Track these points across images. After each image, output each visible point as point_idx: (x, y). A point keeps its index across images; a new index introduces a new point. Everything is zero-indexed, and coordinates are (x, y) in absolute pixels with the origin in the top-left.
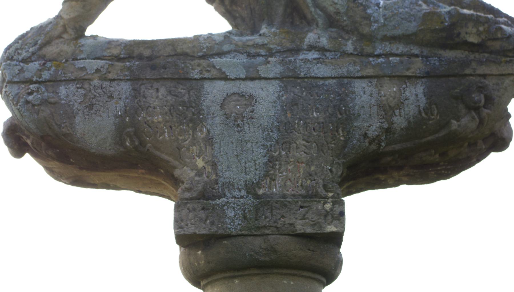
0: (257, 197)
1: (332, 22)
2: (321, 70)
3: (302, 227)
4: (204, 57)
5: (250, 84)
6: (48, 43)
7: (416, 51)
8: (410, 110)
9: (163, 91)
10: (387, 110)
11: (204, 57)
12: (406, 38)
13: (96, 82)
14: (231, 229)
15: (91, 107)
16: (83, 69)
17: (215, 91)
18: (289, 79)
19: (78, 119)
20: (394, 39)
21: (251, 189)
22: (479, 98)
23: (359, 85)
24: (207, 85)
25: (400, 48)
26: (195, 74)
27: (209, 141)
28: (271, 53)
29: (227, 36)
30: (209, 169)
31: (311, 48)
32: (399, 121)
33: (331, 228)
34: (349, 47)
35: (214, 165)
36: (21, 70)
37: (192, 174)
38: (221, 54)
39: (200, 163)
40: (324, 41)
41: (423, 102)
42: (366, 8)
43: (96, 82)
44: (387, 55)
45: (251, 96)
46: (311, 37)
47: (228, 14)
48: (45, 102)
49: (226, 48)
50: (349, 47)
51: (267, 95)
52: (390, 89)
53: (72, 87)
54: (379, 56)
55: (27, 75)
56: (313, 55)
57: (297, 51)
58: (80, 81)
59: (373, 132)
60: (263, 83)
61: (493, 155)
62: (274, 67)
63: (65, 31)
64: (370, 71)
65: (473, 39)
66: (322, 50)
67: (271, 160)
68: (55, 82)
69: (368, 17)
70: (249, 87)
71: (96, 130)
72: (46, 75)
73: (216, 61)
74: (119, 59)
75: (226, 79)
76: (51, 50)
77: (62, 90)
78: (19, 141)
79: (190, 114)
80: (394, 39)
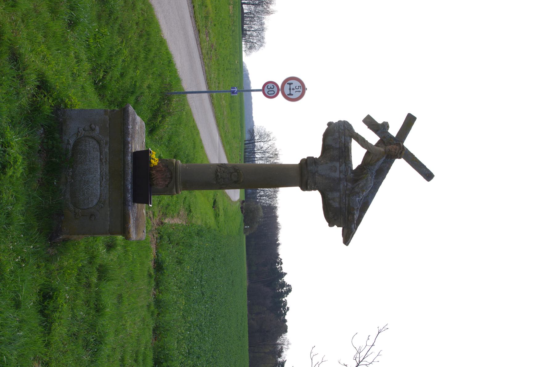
1: (353, 188)
2: (342, 186)
3: (309, 181)
12: (349, 204)
17: (337, 164)
18: (340, 179)
21: (317, 172)
23: (338, 194)
25: (347, 203)
27: (327, 163)
28: (345, 176)
29: (351, 167)
32: (331, 202)
33: (308, 187)
34: (347, 192)
38: (346, 166)
40: (349, 187)
46: (350, 184)
47: (359, 167)
50: (347, 192)
51: (337, 175)
57: (346, 181)
58: (339, 137)
70: (338, 172)
73: (344, 165)
74: (345, 144)
76: (347, 131)
78: (330, 124)
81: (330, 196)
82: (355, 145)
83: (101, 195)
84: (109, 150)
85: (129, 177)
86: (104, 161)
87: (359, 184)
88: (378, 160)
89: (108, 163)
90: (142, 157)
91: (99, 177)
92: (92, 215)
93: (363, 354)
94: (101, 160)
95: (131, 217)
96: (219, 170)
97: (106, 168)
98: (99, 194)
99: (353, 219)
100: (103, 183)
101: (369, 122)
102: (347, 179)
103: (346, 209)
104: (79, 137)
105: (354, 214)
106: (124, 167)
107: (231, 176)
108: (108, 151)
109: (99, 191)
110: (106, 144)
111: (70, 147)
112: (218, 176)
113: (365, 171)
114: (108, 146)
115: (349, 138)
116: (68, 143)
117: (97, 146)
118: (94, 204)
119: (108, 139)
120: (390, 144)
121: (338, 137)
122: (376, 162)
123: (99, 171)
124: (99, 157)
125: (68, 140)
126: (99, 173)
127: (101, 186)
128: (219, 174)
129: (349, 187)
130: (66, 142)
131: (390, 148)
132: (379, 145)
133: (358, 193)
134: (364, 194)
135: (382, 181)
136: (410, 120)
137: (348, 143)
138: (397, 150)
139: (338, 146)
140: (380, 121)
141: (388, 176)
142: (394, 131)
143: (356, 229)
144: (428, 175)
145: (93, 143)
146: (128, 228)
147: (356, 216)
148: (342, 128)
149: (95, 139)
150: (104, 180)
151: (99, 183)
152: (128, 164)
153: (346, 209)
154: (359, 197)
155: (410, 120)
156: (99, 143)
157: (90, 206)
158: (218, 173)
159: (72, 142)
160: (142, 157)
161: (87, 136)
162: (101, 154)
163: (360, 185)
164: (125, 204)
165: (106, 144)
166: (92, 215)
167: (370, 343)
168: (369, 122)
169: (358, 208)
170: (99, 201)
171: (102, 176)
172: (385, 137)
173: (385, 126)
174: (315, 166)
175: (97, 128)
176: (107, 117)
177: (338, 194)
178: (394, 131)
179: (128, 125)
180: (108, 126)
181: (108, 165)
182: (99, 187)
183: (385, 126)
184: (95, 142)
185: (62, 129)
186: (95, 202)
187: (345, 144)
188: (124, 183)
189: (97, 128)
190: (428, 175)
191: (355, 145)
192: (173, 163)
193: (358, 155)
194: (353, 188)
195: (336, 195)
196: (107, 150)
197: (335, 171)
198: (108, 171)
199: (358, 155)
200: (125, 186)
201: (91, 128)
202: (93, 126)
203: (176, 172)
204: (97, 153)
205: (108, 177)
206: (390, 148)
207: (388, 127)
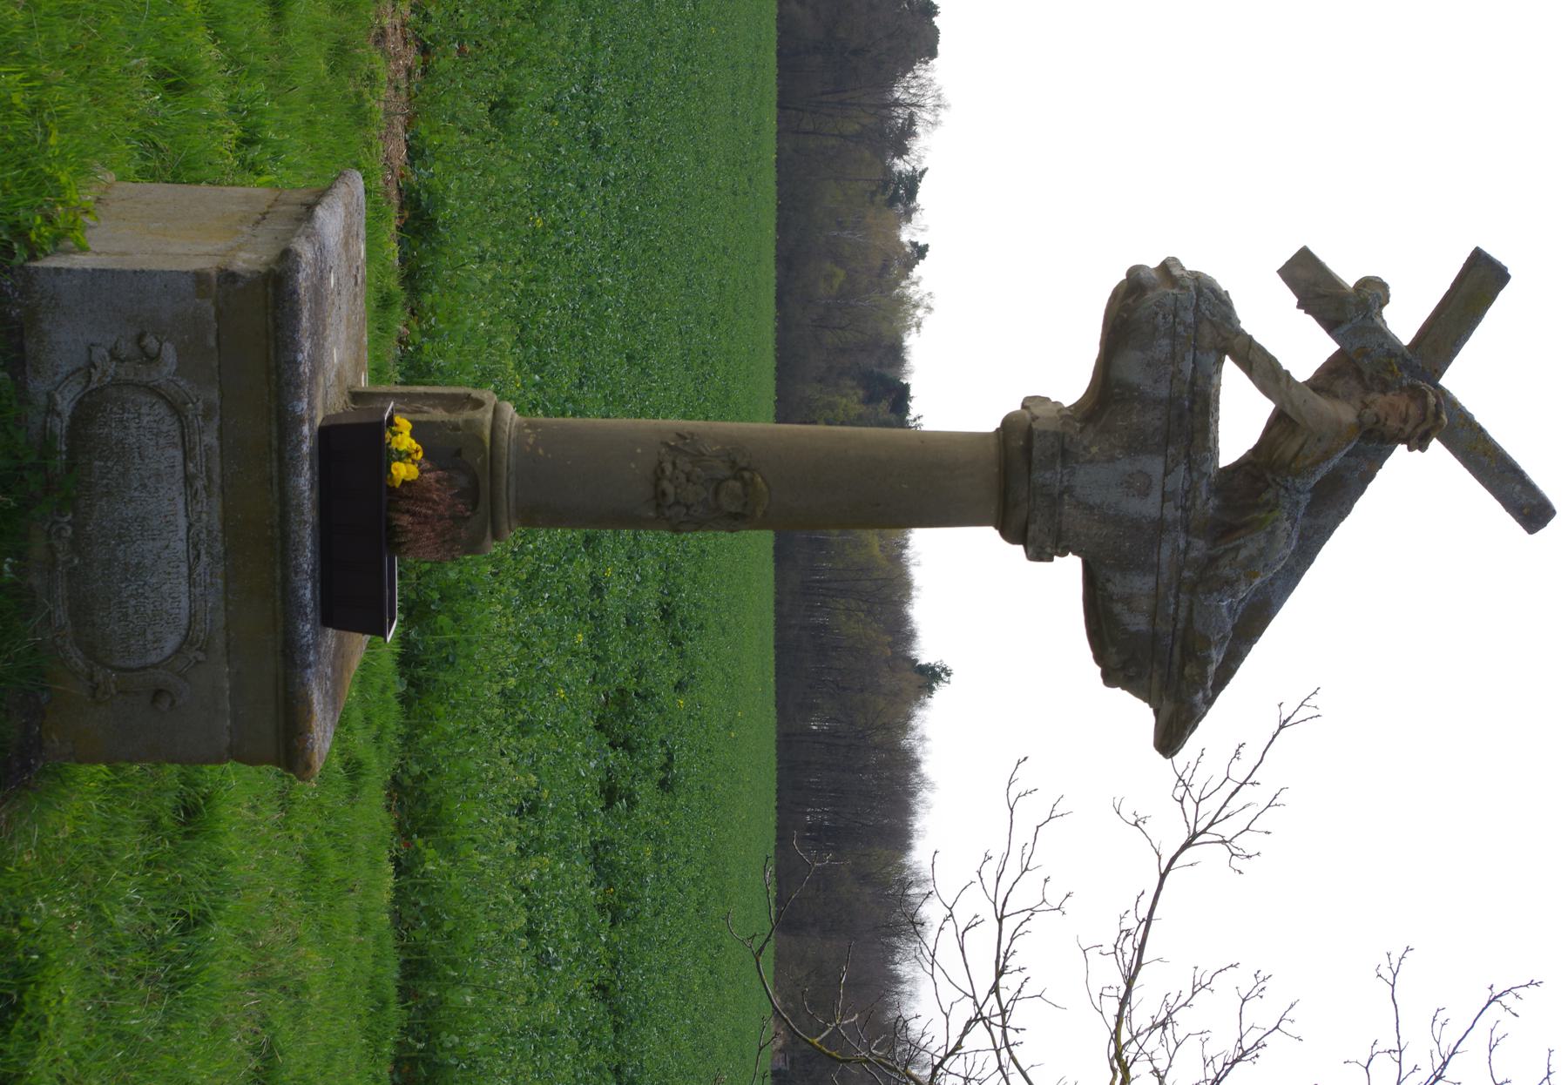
0: (1061, 494)
1: (1212, 561)
2: (1166, 552)
3: (1033, 528)
4: (1188, 455)
5: (1159, 494)
6: (1212, 323)
7: (1179, 626)
8: (1127, 618)
9: (1158, 423)
10: (1128, 600)
11: (1188, 455)
12: (1189, 620)
13: (1171, 368)
14: (1035, 475)
15: (1149, 365)
16: (1183, 359)
17: (1155, 466)
18: (1160, 526)
19: (1139, 354)
20: (1191, 610)
21: (1069, 490)
22: (1132, 672)
23: (1150, 581)
24: (1161, 459)
25: (1182, 614)
26: (1171, 450)
27: (1111, 459)
28: (1185, 509)
30: (1088, 457)
31: (1188, 543)
32: (1118, 608)
34: (1186, 574)
35: (1091, 461)
36: (1186, 309)
37: (1086, 442)
38: (1190, 469)
39: (1094, 449)
40: (1193, 554)
41: (1133, 629)
42: (1219, 591)
43: (1171, 368)
44: (1177, 604)
45: (1147, 495)
48: (1156, 328)
49: (1195, 474)
50: (1186, 574)
51: (1149, 507)
52: (1145, 604)
53: (1168, 349)
54: (1177, 596)
55: (1182, 313)
56: (1182, 545)
57: (1187, 532)
58: (1173, 356)
59: (1110, 586)
60: (1159, 504)
61: (1099, 669)
62: (1172, 513)
63: (1225, 339)
64: (1162, 589)
65: (1187, 670)
66: (1186, 552)
67: (1091, 508)
68: (1173, 335)
69: (1210, 592)
70: (1156, 495)
71: (1131, 368)
72: (1180, 329)
74: (1193, 383)
75: (1166, 474)
76: (1206, 329)
77: (1165, 342)
79: (1136, 445)
80: (1191, 610)
81: (1117, 585)
82: (1232, 376)
83: (192, 616)
84: (220, 438)
85: (307, 558)
86: (199, 484)
87: (1237, 549)
88: (1327, 456)
89: (216, 490)
90: (354, 446)
91: (182, 546)
92: (158, 694)
93: (1210, 807)
94: (188, 480)
95: (317, 708)
96: (668, 468)
97: (211, 512)
98: (184, 614)
99: (1204, 676)
100: (200, 569)
101: (1308, 279)
102: (1193, 504)
103: (1171, 639)
104: (92, 386)
105: (1207, 661)
106: (284, 518)
107: (716, 493)
108: (215, 443)
109: (185, 602)
110: (207, 415)
111: (60, 426)
112: (664, 494)
113: (1268, 495)
114: (215, 424)
115: (1212, 358)
116: (51, 409)
117: (170, 425)
118: (168, 651)
119: (214, 396)
120: (1385, 388)
121: (1164, 326)
122: (1316, 464)
123: (182, 522)
124: (179, 468)
125: (50, 396)
126: (182, 533)
127: (192, 583)
128: (670, 489)
129: (1193, 554)
130: (43, 400)
131: (1386, 387)
132: (1339, 386)
133: (1231, 582)
134: (1257, 582)
135: (1336, 525)
136: (1480, 282)
137: (1210, 377)
138: (1411, 423)
139: (1163, 391)
140: (1349, 276)
141: (1362, 506)
142: (1404, 320)
143: (1209, 702)
144: (1531, 510)
145: (152, 414)
146: (304, 749)
147: (1217, 656)
148: (1189, 318)
149: (162, 397)
150: (204, 558)
151: (184, 569)
152: (299, 505)
153: (1171, 639)
154: (1233, 596)
155: (1480, 282)
156: (177, 409)
157: (153, 658)
158: (666, 484)
159: (65, 404)
160: (354, 446)
161: (128, 383)
162: (187, 456)
163: (1244, 553)
164: (291, 658)
165: (207, 415)
166: (158, 694)
167: (1239, 772)
168: (1308, 279)
169: (1225, 637)
170: (187, 641)
171: (193, 544)
172: (1364, 352)
173: (1373, 293)
174: (1064, 465)
175: (169, 352)
176: (208, 304)
177: (1150, 581)
178: (1404, 320)
179: (297, 348)
180: (212, 342)
181: (217, 503)
182: (184, 588)
183: (1373, 293)
184: (161, 409)
185: (21, 348)
186: (171, 642)
187: (1193, 383)
188: (286, 579)
189: (169, 352)
190: (1531, 510)
191: (1234, 384)
192: (482, 441)
193: (1241, 418)
194: (1212, 561)
195: (1141, 584)
196: (210, 438)
197: (1144, 493)
198: (217, 526)
199: (1241, 418)
200: (288, 592)
201: (143, 349)
202: (151, 342)
203: (494, 476)
204: (171, 452)
205: (219, 548)
206: (1386, 387)
207: (1385, 299)
